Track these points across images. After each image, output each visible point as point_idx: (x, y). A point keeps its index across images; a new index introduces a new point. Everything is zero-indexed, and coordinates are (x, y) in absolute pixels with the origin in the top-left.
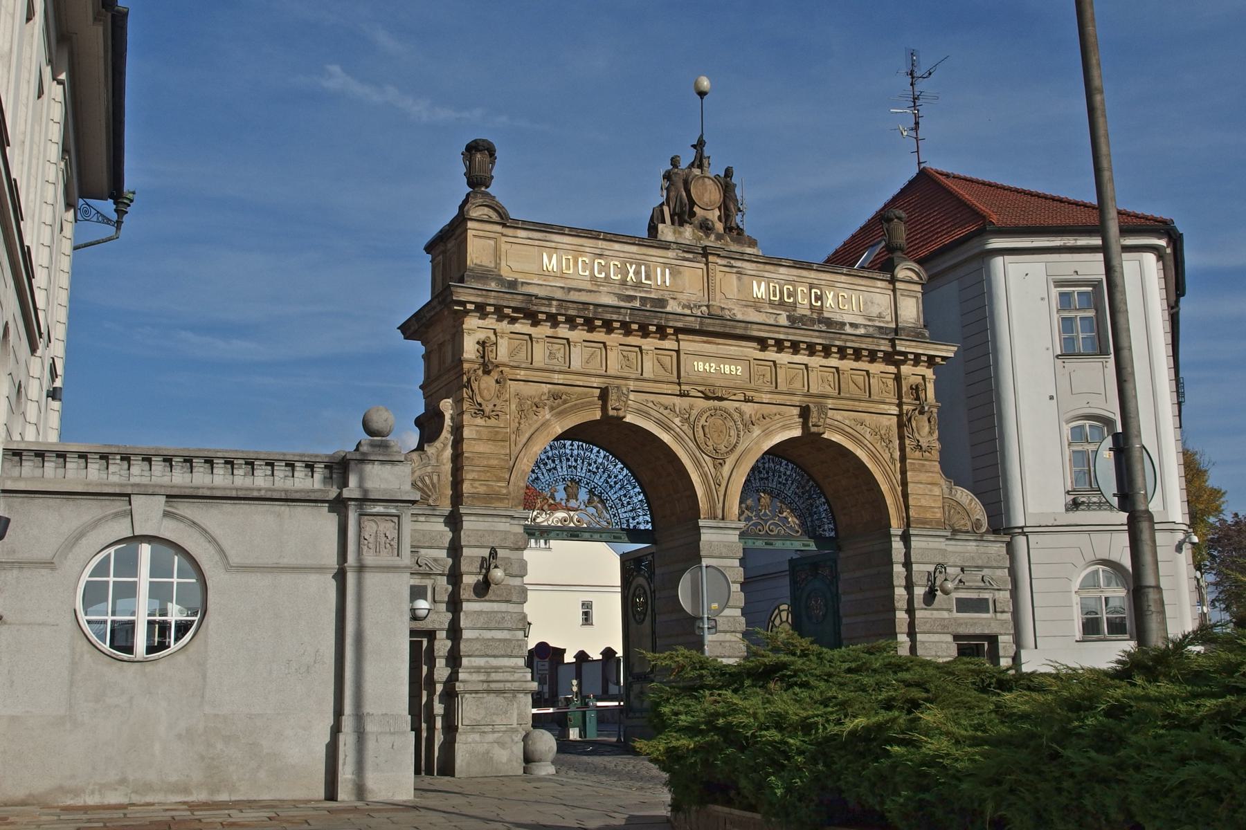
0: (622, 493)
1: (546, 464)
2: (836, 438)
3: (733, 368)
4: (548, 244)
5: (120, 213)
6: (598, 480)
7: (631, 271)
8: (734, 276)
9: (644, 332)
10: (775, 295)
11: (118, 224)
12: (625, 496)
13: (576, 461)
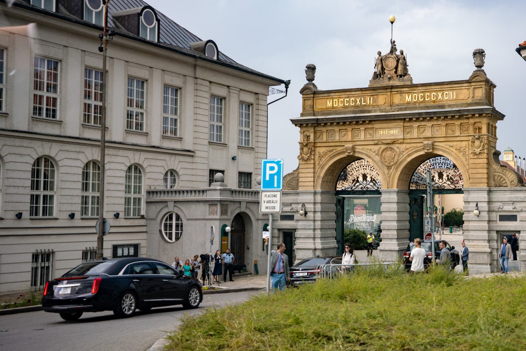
5: (287, 87)
6: (374, 173)
9: (357, 123)
10: (415, 99)
11: (287, 91)
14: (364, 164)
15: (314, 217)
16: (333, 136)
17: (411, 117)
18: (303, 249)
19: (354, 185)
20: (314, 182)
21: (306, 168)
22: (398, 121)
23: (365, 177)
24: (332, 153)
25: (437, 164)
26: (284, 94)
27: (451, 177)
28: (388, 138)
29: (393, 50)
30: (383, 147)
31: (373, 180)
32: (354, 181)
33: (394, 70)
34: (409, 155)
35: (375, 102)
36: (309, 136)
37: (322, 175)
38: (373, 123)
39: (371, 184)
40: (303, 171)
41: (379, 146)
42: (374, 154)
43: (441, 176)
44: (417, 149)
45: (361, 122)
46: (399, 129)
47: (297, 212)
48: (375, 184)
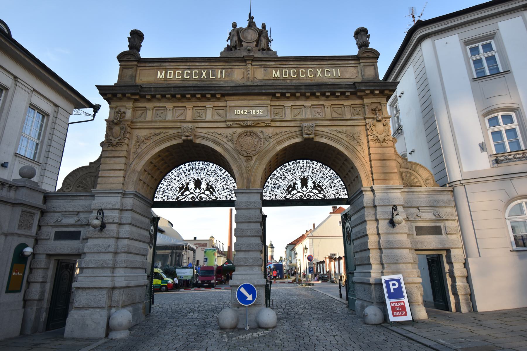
0: (225, 183)
1: (185, 173)
2: (324, 140)
3: (258, 111)
4: (162, 68)
6: (212, 179)
7: (204, 73)
8: (262, 69)
10: (285, 75)
11: (94, 115)
12: (225, 185)
13: (201, 170)
14: (197, 167)
15: (118, 232)
16: (162, 115)
17: (284, 91)
18: (89, 288)
19: (182, 194)
20: (124, 177)
21: (114, 157)
22: (264, 97)
23: (198, 183)
24: (159, 137)
25: (299, 169)
26: (92, 118)
27: (318, 184)
28: (247, 118)
29: (251, 23)
30: (240, 131)
31: (210, 188)
32: (181, 189)
33: (255, 43)
34: (279, 143)
35: (229, 76)
36: (124, 113)
37: (139, 168)
38: (227, 98)
39: (207, 192)
40: (108, 160)
41: (234, 130)
42: (225, 140)
43: (304, 182)
44: (290, 135)
45: (209, 96)
46: (264, 108)
47: (88, 224)
48: (212, 193)
